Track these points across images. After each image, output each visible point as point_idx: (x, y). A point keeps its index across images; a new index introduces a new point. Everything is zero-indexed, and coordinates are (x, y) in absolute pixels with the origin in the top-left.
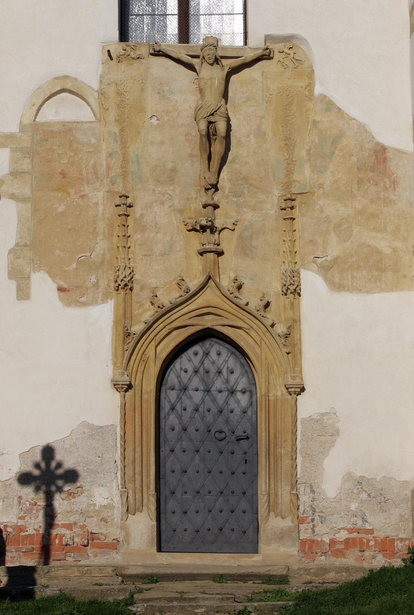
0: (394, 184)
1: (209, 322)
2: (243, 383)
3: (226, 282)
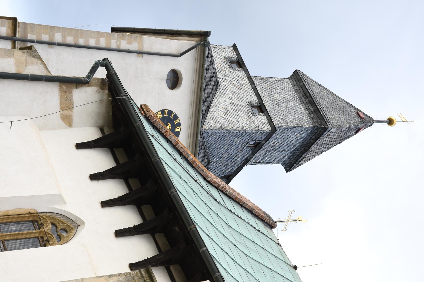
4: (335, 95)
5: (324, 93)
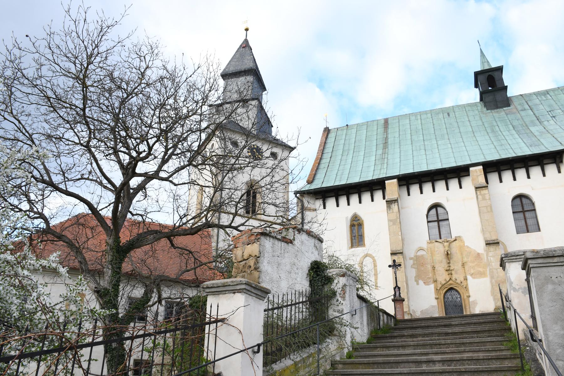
0: (482, 259)
1: (451, 286)
2: (459, 296)
3: (453, 279)
4: (233, 57)
5: (233, 63)
